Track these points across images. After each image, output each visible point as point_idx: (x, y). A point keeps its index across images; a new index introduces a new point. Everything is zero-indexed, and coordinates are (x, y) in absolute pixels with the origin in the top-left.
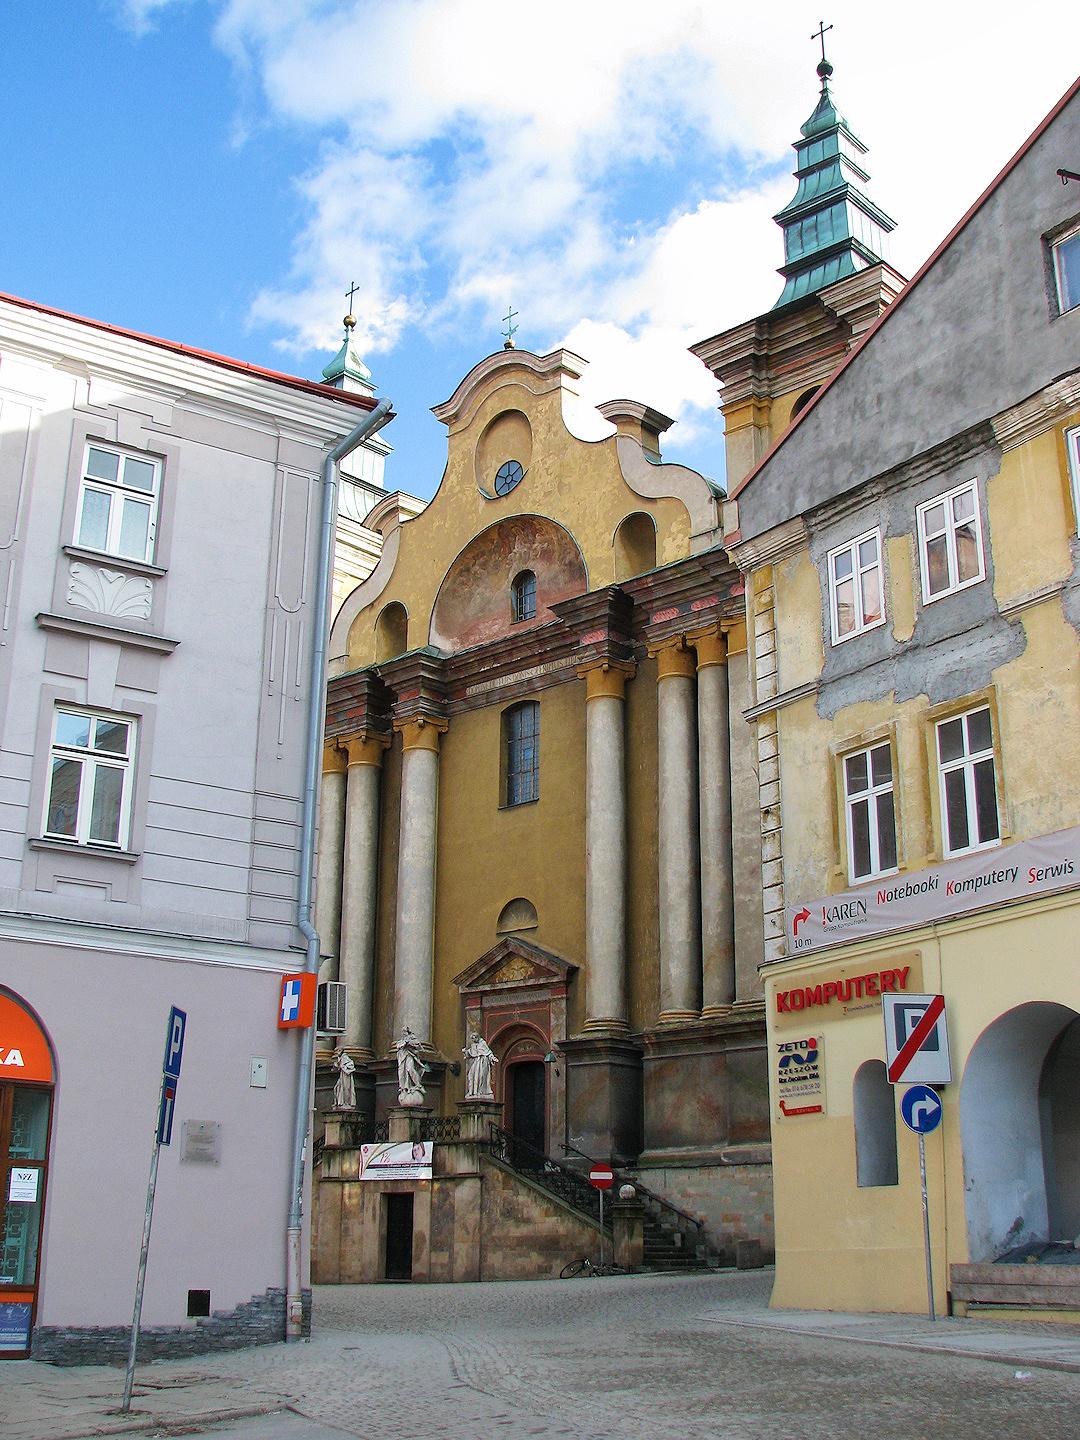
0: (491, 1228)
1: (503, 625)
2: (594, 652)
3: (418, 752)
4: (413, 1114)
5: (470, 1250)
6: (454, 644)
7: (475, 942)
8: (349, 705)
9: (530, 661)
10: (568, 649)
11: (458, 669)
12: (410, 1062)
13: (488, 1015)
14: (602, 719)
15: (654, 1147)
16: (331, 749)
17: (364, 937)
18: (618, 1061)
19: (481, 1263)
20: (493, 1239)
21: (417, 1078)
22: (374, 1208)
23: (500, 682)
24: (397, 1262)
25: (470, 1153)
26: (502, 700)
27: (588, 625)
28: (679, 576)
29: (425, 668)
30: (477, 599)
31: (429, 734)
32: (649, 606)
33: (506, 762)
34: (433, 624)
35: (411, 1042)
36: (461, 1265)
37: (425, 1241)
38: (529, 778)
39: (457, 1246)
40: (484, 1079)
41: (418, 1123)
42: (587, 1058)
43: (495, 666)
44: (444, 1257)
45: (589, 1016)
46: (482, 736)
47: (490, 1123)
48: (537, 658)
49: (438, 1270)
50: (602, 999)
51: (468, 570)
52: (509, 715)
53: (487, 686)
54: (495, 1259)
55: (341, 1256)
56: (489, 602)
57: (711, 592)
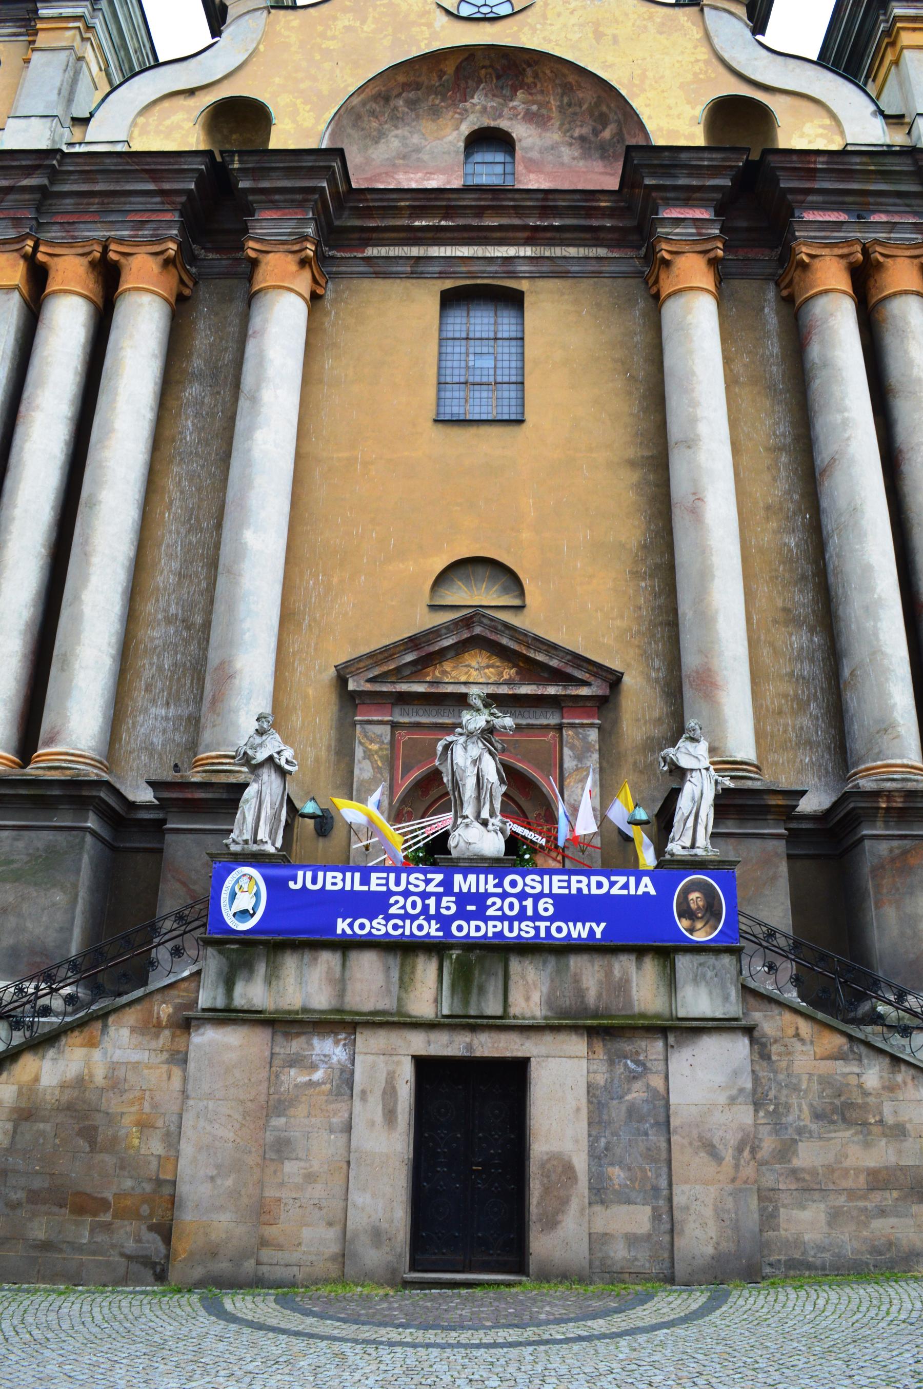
0: (786, 1151)
2: (694, 231)
3: (293, 297)
5: (730, 1203)
8: (137, 202)
9: (511, 234)
11: (368, 212)
13: (404, 736)
16: (85, 261)
17: (127, 563)
20: (794, 1172)
23: (436, 251)
26: (442, 275)
27: (682, 195)
28: (872, 168)
29: (332, 181)
30: (395, 143)
31: (303, 281)
32: (800, 197)
42: (730, 823)
43: (443, 223)
51: (387, 99)
53: (415, 251)
57: (907, 209)
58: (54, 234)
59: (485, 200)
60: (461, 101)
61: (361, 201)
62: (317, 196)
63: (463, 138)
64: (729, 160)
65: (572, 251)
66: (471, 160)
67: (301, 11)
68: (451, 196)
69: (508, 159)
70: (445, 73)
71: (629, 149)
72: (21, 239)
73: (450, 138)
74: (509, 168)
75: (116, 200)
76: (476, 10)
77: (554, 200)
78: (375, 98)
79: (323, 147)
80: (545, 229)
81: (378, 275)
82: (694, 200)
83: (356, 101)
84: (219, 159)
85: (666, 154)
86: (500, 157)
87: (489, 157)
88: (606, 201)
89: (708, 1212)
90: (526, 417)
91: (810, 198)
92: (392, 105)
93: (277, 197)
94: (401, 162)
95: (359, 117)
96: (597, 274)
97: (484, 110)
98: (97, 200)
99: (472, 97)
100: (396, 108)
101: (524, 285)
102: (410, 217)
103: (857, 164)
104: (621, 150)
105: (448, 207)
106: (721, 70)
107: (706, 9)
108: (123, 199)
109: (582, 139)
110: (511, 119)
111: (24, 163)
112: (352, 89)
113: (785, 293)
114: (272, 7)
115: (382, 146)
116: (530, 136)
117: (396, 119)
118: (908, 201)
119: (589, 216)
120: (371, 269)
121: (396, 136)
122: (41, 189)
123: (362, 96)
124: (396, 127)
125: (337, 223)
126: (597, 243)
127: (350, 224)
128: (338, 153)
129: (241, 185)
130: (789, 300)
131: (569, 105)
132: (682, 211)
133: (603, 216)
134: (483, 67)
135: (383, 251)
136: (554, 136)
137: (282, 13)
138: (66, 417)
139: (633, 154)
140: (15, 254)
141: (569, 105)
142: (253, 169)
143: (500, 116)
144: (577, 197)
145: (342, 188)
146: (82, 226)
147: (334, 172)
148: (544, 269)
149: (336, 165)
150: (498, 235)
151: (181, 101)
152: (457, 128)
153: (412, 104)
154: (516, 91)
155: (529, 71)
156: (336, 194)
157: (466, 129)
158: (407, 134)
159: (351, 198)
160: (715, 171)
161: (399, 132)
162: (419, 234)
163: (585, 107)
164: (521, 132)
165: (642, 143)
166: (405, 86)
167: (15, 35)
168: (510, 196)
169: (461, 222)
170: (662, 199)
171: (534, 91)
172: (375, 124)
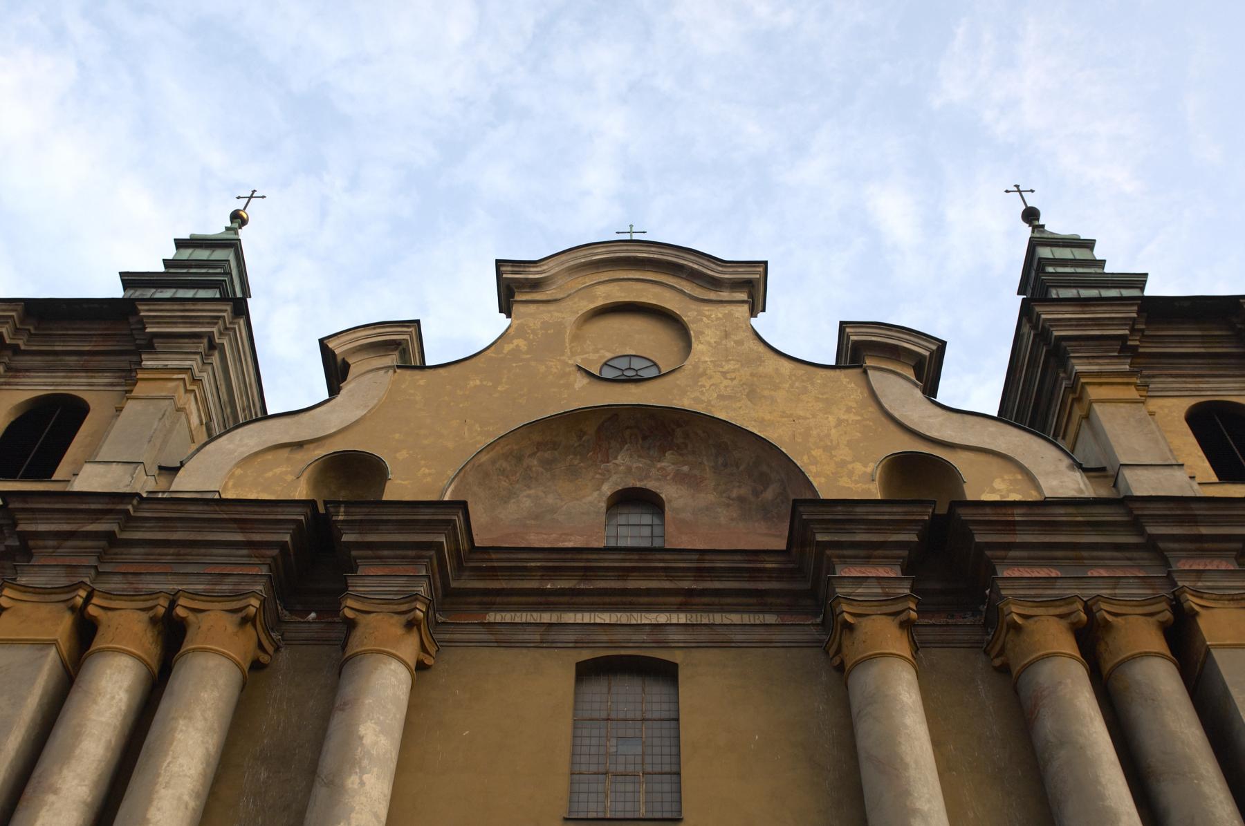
2: (879, 591)
3: (395, 666)
9: (661, 599)
16: (145, 616)
26: (578, 645)
27: (862, 553)
31: (409, 648)
48: (679, 599)
51: (519, 459)
58: (113, 586)
59: (630, 560)
60: (603, 462)
61: (483, 560)
62: (432, 553)
63: (605, 498)
64: (912, 513)
65: (735, 618)
66: (614, 522)
67: (428, 372)
68: (590, 556)
69: (657, 521)
70: (585, 433)
71: (796, 503)
72: (73, 588)
73: (590, 499)
74: (657, 531)
75: (195, 551)
76: (619, 373)
77: (711, 561)
79: (446, 498)
80: (703, 593)
81: (501, 644)
82: (876, 558)
83: (484, 458)
84: (322, 510)
85: (840, 508)
86: (647, 519)
87: (634, 519)
88: (771, 562)
90: (684, 814)
91: (1012, 554)
92: (525, 465)
93: (386, 553)
94: (533, 522)
96: (766, 644)
97: (629, 469)
98: (172, 551)
99: (616, 458)
100: (529, 468)
101: (676, 657)
102: (542, 578)
103: (1061, 515)
104: (786, 509)
105: (586, 569)
106: (892, 427)
107: (870, 372)
108: (203, 551)
109: (741, 500)
110: (659, 480)
111: (93, 506)
112: (480, 447)
113: (997, 662)
114: (398, 367)
115: (512, 506)
116: (681, 497)
118: (1128, 554)
119: (752, 579)
120: (492, 637)
121: (528, 496)
122: (110, 536)
123: (492, 454)
124: (529, 488)
125: (454, 584)
126: (764, 608)
127: (468, 583)
128: (463, 506)
129: (345, 538)
130: (1004, 670)
131: (725, 465)
132: (863, 569)
133: (770, 579)
134: (627, 428)
135: (508, 617)
136: (708, 497)
137: (408, 373)
138: (84, 802)
139: (801, 509)
140: (62, 605)
141: (725, 465)
142: (361, 521)
143: (647, 477)
144: (739, 557)
145: (464, 545)
146: (149, 578)
147: (455, 527)
148: (702, 638)
149: (458, 519)
151: (285, 453)
152: (599, 489)
153: (548, 464)
154: (664, 453)
155: (679, 432)
156: (457, 553)
157: (607, 489)
158: (541, 494)
159: (473, 557)
160: (898, 525)
161: (532, 492)
162: (552, 599)
163: (741, 468)
164: (670, 493)
165: (809, 496)
166: (540, 446)
167: (112, 385)
168: (659, 557)
170: (839, 557)
171: (685, 451)
172: (505, 484)
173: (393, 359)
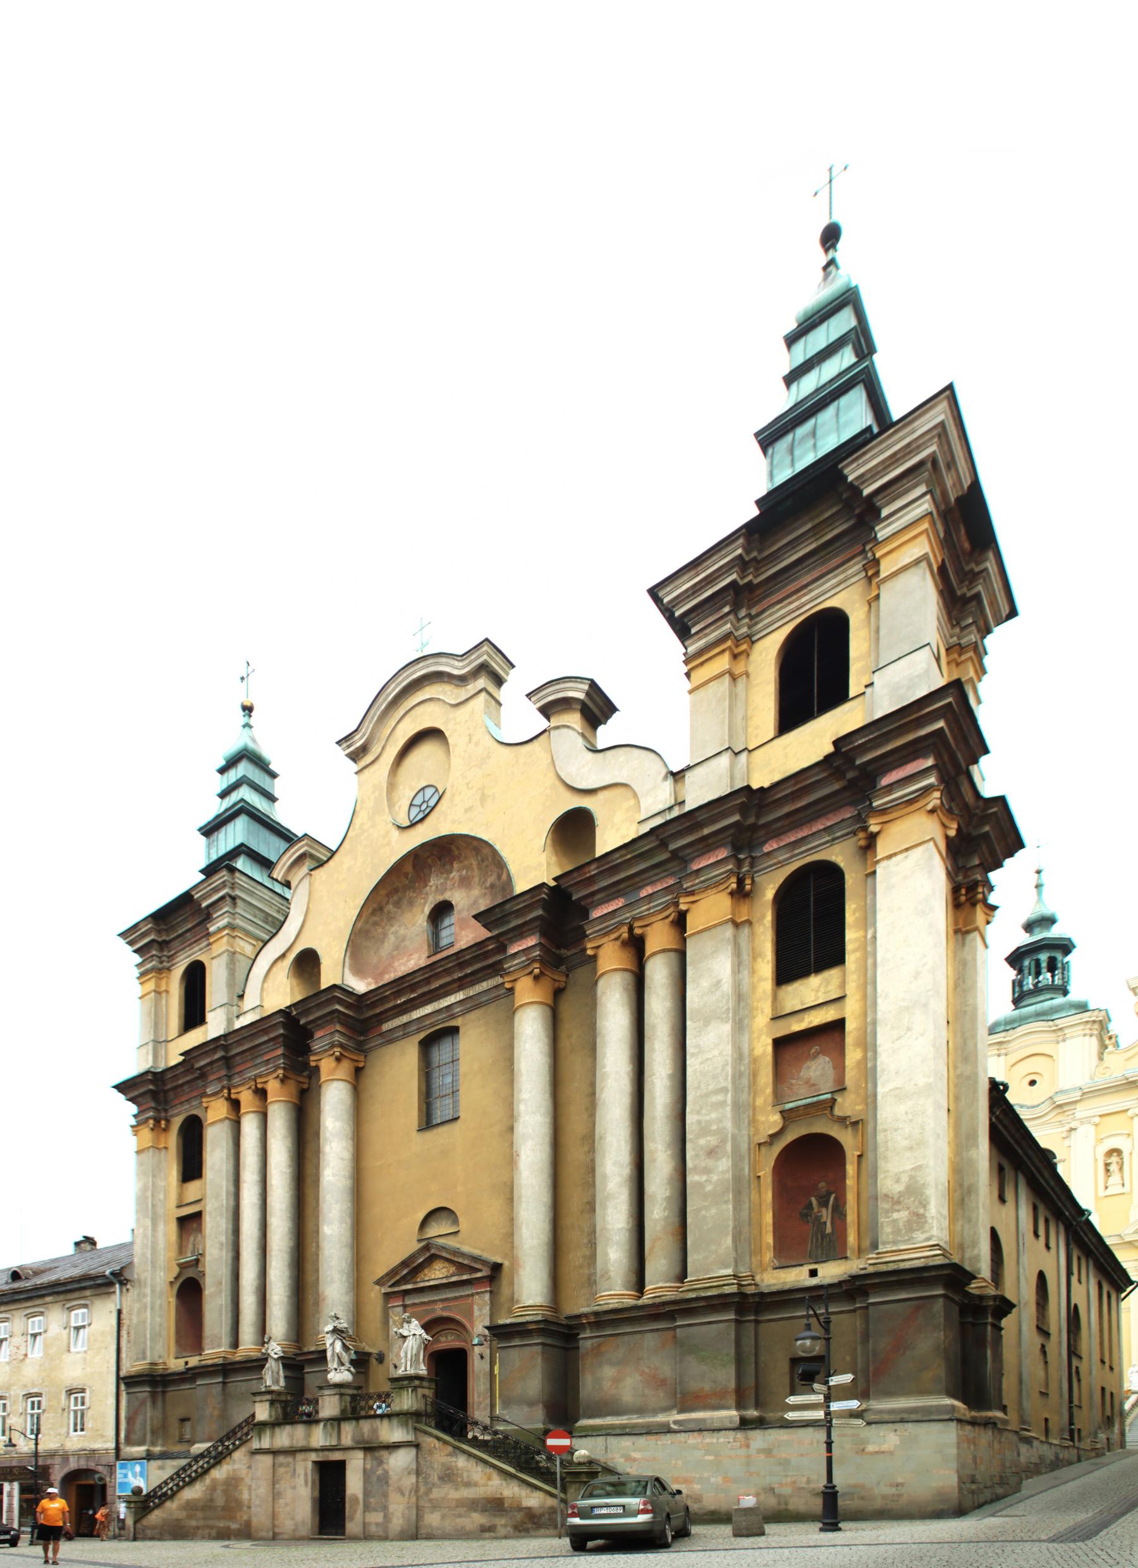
1: (419, 959)
4: (343, 1391)
6: (369, 984)
7: (395, 1245)
9: (449, 988)
10: (496, 969)
11: (374, 1005)
12: (338, 1346)
14: (530, 1028)
15: (590, 1417)
18: (549, 1341)
19: (417, 1522)
21: (346, 1358)
22: (306, 1474)
23: (416, 1014)
24: (331, 1517)
25: (405, 1424)
26: (419, 1030)
29: (340, 1001)
30: (392, 938)
33: (424, 1089)
34: (347, 964)
35: (339, 1326)
36: (397, 1523)
37: (358, 1503)
38: (448, 1101)
39: (392, 1508)
40: (417, 1355)
41: (348, 1399)
44: (376, 1517)
45: (518, 1302)
46: (399, 1065)
47: (424, 1396)
49: (373, 1529)
50: (530, 1289)
51: (381, 909)
52: (427, 1045)
53: (405, 1019)
54: (433, 1519)
55: (274, 1516)
56: (404, 940)
65: (485, 985)
78: (374, 913)
80: (466, 976)
89: (400, 1515)
90: (462, 1114)
95: (367, 932)
100: (389, 912)
117: (391, 919)
124: (392, 926)
150: (442, 991)
161: (393, 929)
166: (389, 895)
169: (420, 991)
172: (380, 930)
173: (308, 864)
